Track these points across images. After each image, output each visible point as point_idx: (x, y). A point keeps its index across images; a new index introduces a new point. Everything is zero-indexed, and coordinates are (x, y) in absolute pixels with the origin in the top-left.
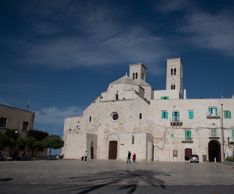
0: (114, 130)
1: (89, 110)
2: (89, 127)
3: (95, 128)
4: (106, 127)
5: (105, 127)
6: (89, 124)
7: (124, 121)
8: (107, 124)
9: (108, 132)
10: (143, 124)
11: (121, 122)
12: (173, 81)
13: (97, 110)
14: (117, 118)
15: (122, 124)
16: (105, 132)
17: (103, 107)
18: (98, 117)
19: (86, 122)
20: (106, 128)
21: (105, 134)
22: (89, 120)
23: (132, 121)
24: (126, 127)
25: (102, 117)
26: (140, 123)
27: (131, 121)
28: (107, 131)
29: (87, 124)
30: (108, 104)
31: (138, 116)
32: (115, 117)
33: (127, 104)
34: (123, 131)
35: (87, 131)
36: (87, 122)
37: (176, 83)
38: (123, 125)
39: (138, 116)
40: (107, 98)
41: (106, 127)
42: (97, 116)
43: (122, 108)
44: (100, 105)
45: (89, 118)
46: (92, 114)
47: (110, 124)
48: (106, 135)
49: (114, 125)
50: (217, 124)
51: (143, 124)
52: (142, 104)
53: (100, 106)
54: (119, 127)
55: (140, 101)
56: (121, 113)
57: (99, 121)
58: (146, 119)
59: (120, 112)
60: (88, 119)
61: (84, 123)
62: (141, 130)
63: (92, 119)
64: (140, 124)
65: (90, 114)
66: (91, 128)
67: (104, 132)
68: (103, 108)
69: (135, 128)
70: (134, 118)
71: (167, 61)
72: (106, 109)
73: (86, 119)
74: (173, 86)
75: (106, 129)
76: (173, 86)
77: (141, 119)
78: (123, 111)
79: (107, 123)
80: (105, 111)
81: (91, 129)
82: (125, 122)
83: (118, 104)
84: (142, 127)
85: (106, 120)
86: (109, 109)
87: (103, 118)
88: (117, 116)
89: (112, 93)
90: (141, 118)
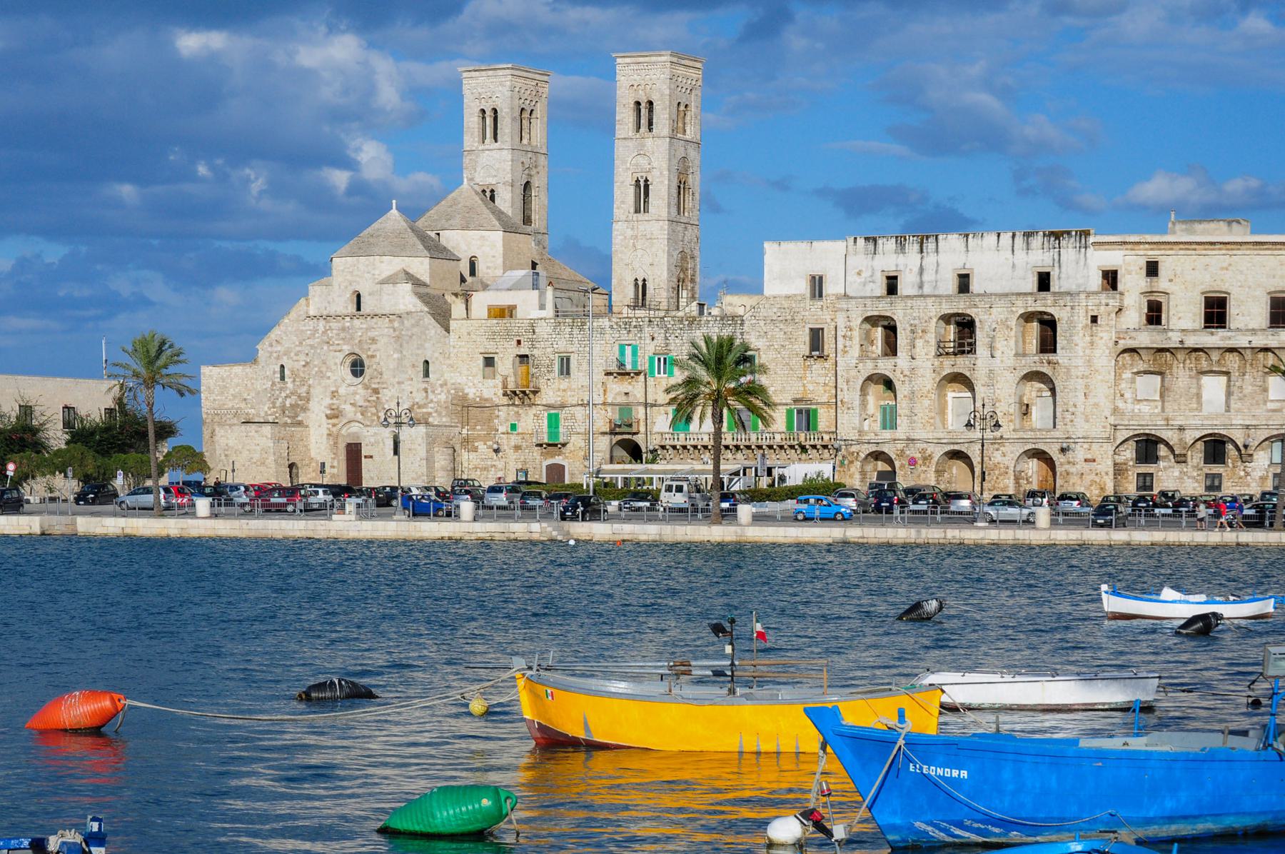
0: (354, 409)
1: (274, 343)
2: (280, 400)
3: (299, 402)
4: (332, 399)
5: (328, 401)
6: (281, 389)
7: (383, 383)
8: (333, 392)
9: (337, 417)
10: (433, 392)
11: (374, 386)
12: (643, 161)
13: (301, 343)
14: (362, 373)
15: (376, 391)
16: (328, 417)
17: (317, 335)
18: (304, 366)
19: (270, 383)
20: (333, 404)
21: (330, 421)
22: (278, 375)
23: (403, 383)
24: (387, 401)
25: (316, 369)
26: (426, 390)
27: (399, 383)
28: (336, 412)
29: (272, 390)
30: (331, 324)
31: (419, 369)
32: (357, 368)
33: (386, 330)
34: (380, 414)
35: (277, 412)
36: (273, 384)
37: (656, 173)
38: (379, 396)
39: (419, 369)
40: (329, 302)
41: (332, 399)
42: (304, 363)
43: (374, 340)
44: (307, 328)
45: (278, 369)
46: (285, 358)
47: (342, 391)
48: (334, 425)
49: (355, 393)
50: (636, 392)
51: (433, 392)
52: (427, 332)
53: (309, 332)
54: (369, 401)
55: (421, 322)
56: (373, 356)
57: (311, 382)
58: (442, 379)
59: (369, 353)
60: (274, 373)
61: (264, 387)
62: (430, 410)
63: (287, 372)
64: (424, 395)
65: (278, 358)
66: (288, 403)
67: (327, 416)
68: (318, 338)
69: (413, 405)
70: (410, 372)
71: (619, 60)
72: (328, 343)
73: (268, 373)
74: (642, 184)
75: (333, 407)
76: (642, 184)
77: (427, 379)
78: (378, 350)
79: (334, 389)
80: (325, 348)
81: (288, 405)
82: (385, 386)
83: (361, 326)
84: (432, 401)
85: (329, 378)
86: (336, 342)
87: (321, 372)
88: (362, 365)
89: (342, 287)
90: (426, 374)
